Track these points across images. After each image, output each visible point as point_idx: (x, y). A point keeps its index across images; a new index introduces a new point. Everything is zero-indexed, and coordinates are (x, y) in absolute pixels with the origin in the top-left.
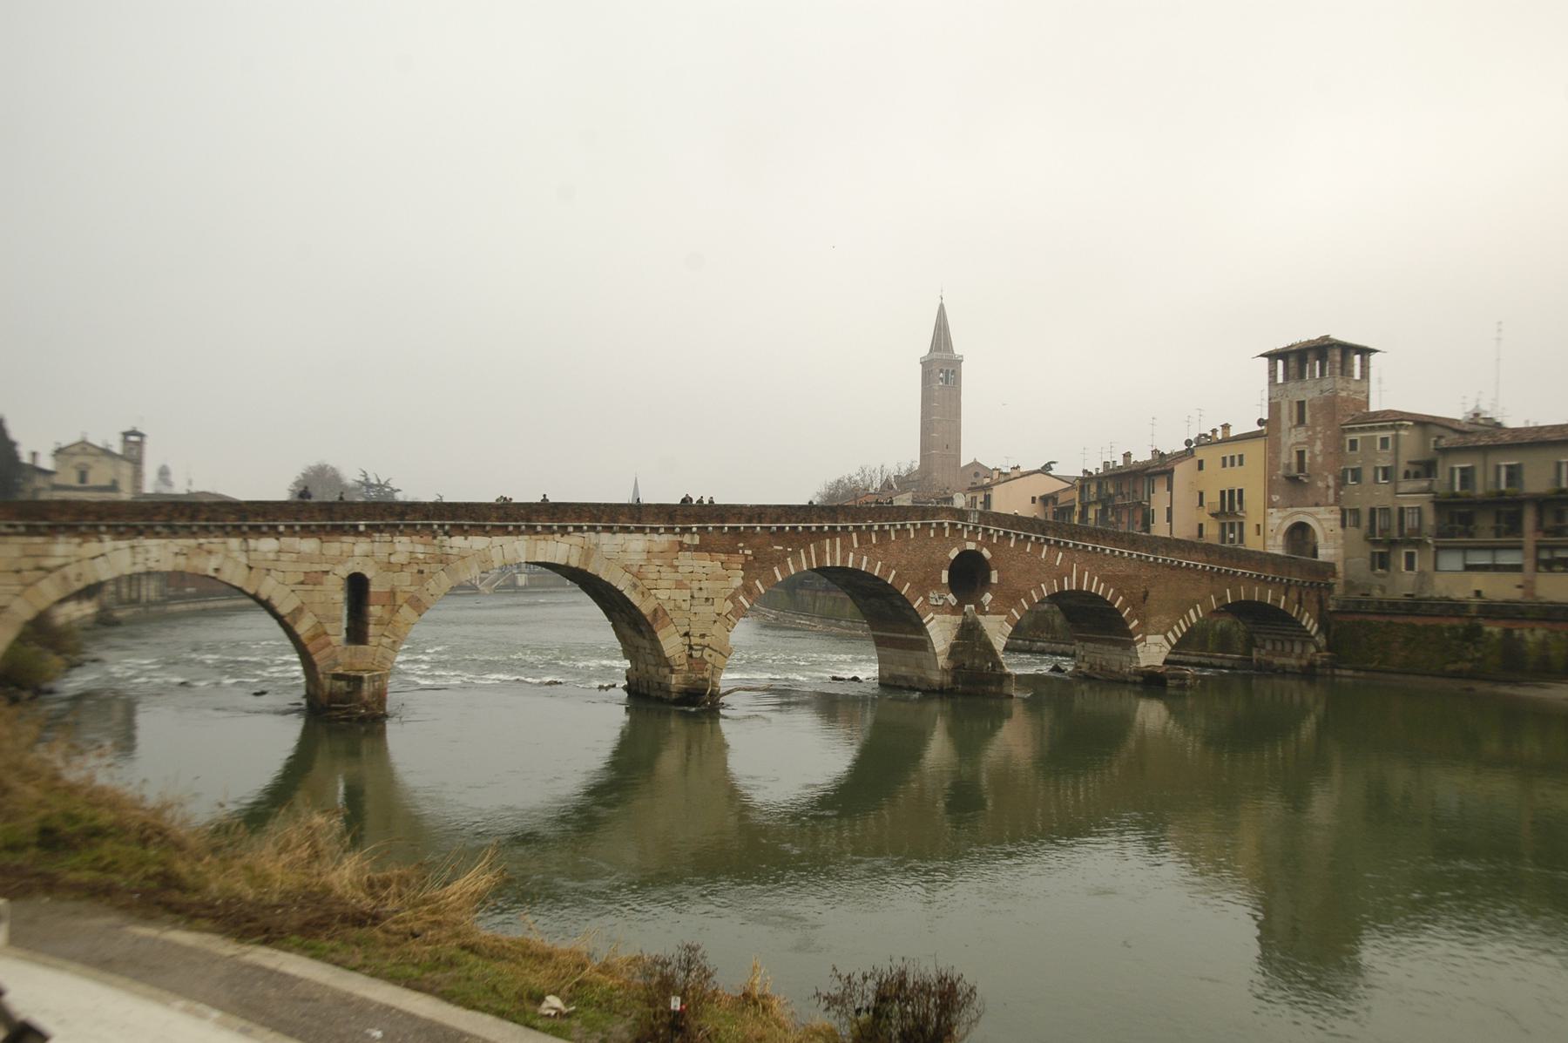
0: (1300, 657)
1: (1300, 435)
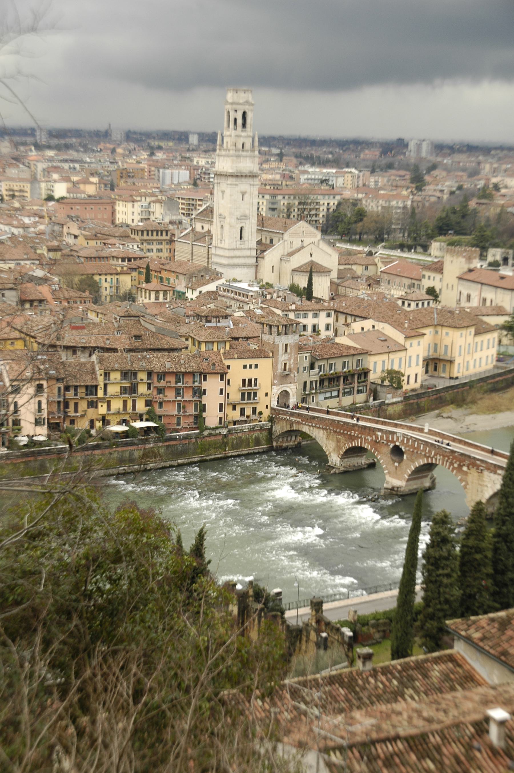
0: (294, 441)
1: (286, 357)
